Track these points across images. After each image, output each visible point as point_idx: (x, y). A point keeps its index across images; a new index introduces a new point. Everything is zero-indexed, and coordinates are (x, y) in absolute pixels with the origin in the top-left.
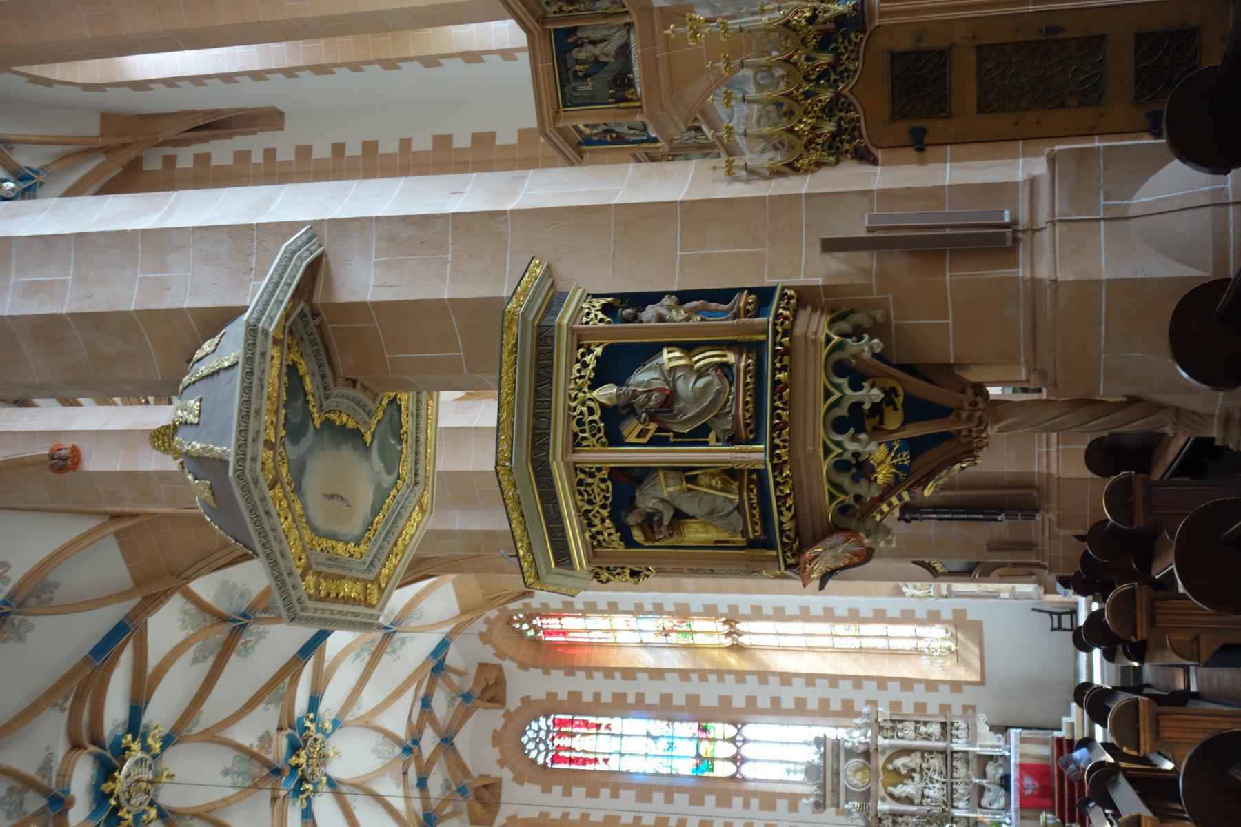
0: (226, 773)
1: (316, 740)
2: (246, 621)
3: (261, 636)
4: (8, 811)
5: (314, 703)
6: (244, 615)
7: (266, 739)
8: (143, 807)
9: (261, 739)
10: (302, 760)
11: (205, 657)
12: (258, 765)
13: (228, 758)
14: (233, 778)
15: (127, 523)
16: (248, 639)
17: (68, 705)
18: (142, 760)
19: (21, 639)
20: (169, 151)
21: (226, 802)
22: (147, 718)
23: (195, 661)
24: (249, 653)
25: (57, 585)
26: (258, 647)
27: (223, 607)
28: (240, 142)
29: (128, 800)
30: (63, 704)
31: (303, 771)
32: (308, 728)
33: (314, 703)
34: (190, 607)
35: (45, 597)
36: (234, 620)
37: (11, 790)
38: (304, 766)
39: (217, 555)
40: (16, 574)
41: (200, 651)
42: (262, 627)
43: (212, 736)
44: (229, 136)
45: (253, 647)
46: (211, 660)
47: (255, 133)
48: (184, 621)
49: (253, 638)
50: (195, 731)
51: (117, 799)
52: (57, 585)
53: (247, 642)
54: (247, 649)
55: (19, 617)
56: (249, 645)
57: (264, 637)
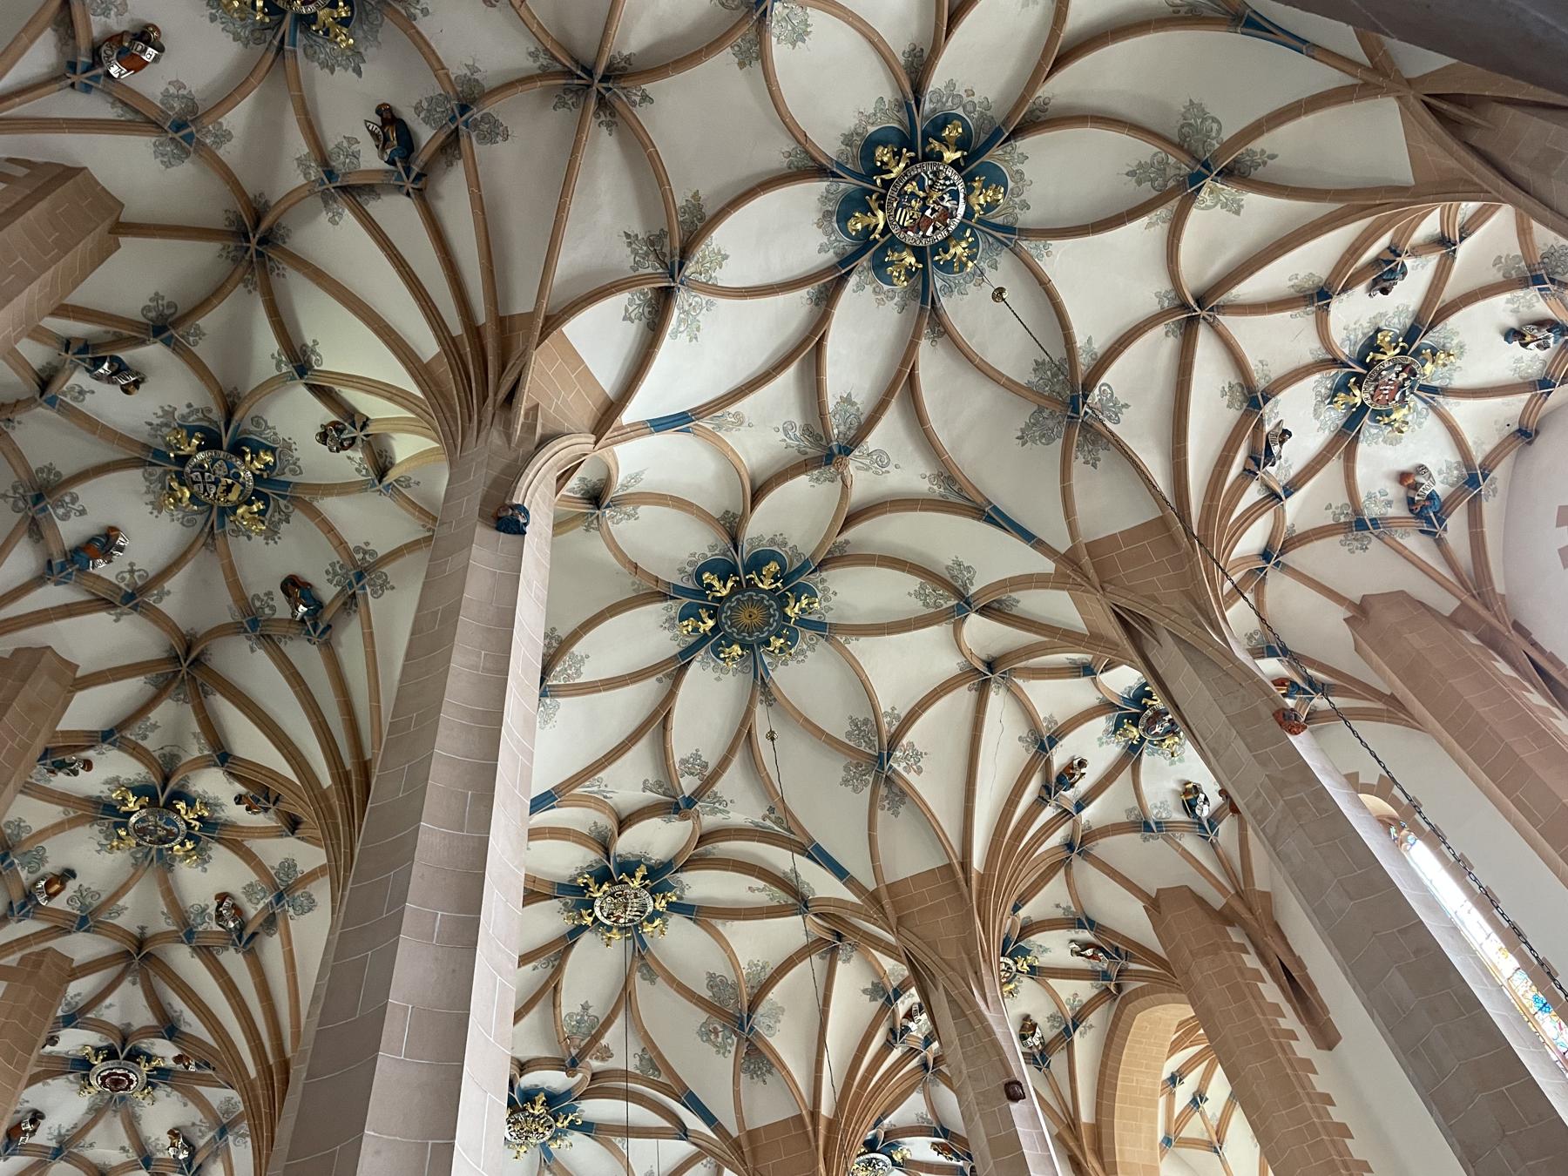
0: (585, 1007)
1: (550, 1127)
2: (747, 1030)
3: (721, 1049)
4: (688, 762)
5: (588, 1128)
6: (752, 1029)
7: (606, 1054)
8: (597, 910)
9: (607, 1048)
10: (539, 1109)
11: (711, 987)
12: (583, 1044)
13: (598, 1011)
14: (578, 1014)
15: (960, 875)
16: (720, 1034)
17: (768, 823)
18: (644, 912)
19: (846, 782)
20: (1251, 949)
21: (555, 1004)
22: (677, 921)
23: (712, 977)
24: (702, 1037)
25: (896, 814)
26: (707, 1045)
27: (762, 1009)
28: (1286, 1008)
29: (612, 895)
30: (770, 818)
31: (525, 1109)
32: (566, 1118)
33: (588, 1128)
34: (769, 971)
35: (885, 803)
36: (749, 1017)
37: (705, 766)
38: (531, 1111)
39: (935, 958)
40: (911, 777)
41: (721, 981)
42: (733, 1049)
43: (625, 998)
44: (1289, 1000)
45: (709, 1040)
46: (706, 994)
47: (1303, 1023)
48: (756, 965)
49: (720, 1040)
50: (638, 975)
51: (621, 882)
52: (896, 814)
53: (716, 1032)
54: (707, 1033)
55: (871, 780)
56: (712, 1037)
57: (718, 1052)
